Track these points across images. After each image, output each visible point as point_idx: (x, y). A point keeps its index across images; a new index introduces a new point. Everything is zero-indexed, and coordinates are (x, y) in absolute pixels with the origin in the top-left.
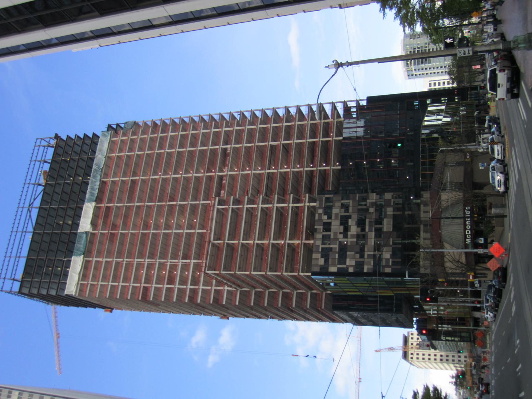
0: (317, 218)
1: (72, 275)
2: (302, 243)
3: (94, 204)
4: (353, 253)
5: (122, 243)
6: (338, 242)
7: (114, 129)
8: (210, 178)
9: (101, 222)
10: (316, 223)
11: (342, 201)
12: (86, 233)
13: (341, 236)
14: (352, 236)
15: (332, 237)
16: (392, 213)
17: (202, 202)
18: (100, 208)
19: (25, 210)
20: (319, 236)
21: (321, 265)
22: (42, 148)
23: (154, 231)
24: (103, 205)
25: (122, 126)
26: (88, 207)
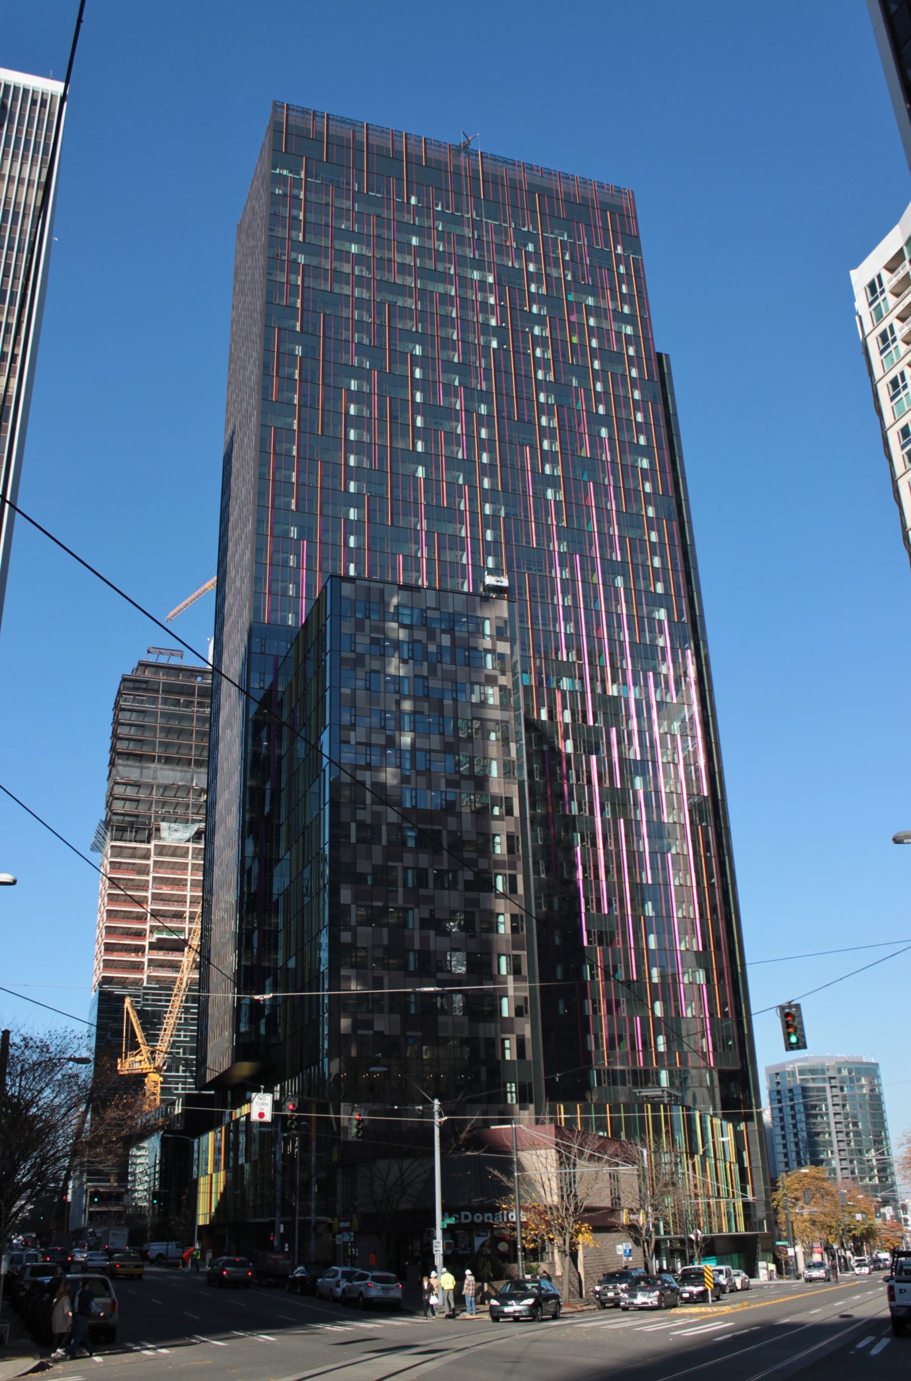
4: (385, 942)
6: (411, 906)
13: (426, 915)
14: (425, 940)
15: (422, 891)
16: (481, 1035)
20: (424, 860)
21: (355, 863)
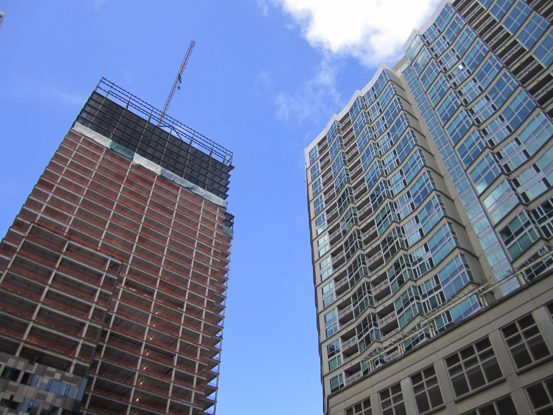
0: (49, 369)
1: (93, 133)
2: (21, 341)
3: (159, 173)
5: (112, 183)
7: (229, 220)
8: (154, 282)
9: (139, 173)
10: (42, 366)
11: (60, 410)
12: (133, 158)
15: (12, 383)
17: (129, 266)
18: (154, 178)
19: (171, 124)
20: (21, 365)
22: (224, 154)
23: (112, 213)
24: (155, 180)
25: (231, 228)
26: (158, 168)
